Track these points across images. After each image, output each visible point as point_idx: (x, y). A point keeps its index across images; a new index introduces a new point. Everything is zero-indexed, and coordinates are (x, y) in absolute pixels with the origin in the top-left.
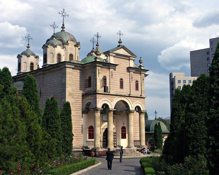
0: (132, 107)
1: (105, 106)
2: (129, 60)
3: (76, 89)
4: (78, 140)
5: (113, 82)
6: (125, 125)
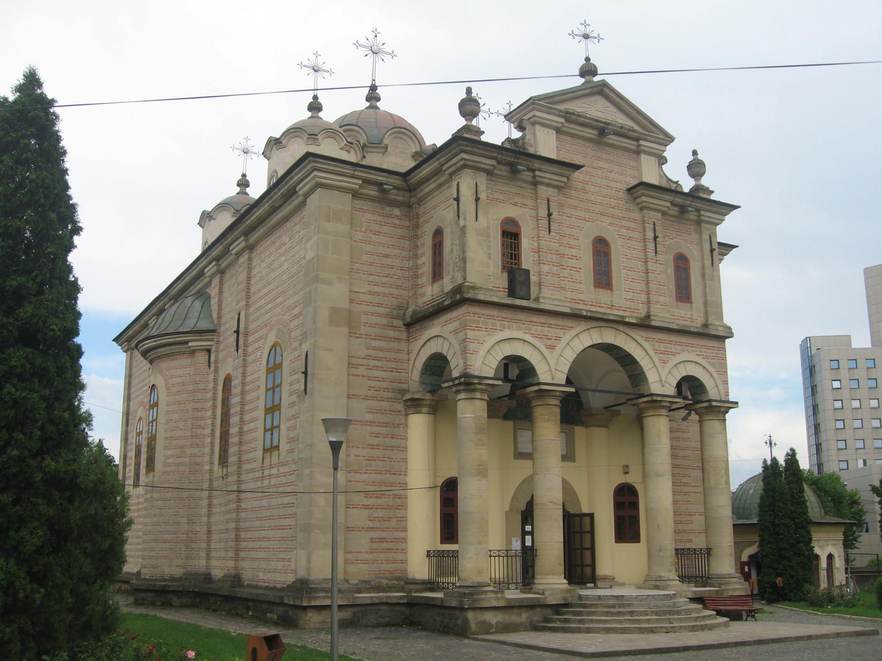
0: (661, 379)
1: (517, 371)
2: (638, 152)
3: (370, 293)
4: (385, 545)
5: (557, 253)
6: (633, 479)
